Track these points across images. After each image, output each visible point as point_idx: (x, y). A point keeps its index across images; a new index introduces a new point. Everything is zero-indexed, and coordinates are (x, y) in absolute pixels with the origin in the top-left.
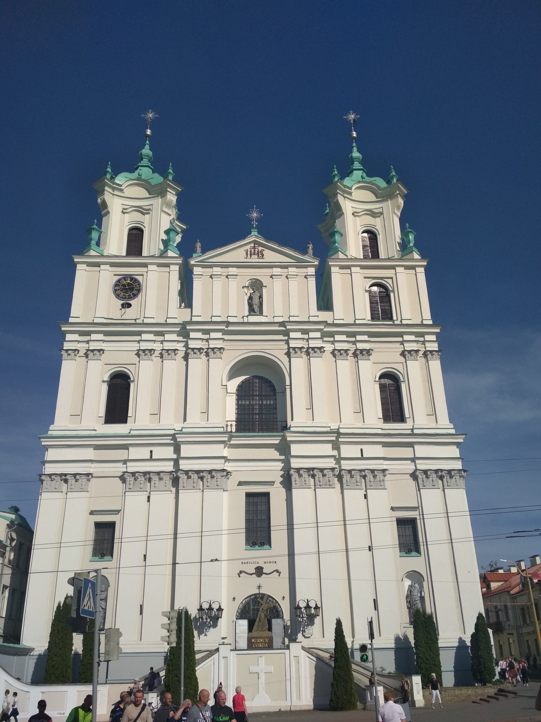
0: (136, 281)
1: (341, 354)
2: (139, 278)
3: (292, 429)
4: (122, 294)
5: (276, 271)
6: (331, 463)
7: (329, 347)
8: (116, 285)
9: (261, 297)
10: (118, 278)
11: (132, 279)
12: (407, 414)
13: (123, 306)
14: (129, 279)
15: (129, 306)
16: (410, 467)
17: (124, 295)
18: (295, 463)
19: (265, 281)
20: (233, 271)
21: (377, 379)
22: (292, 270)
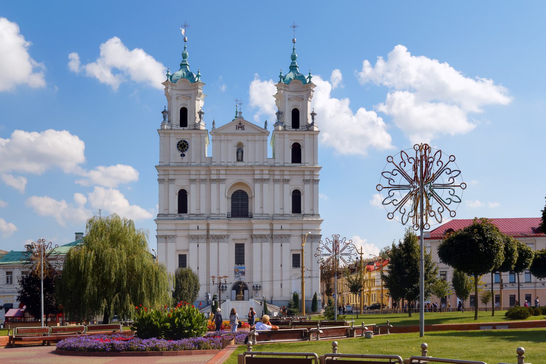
0: (186, 142)
1: (277, 181)
2: (187, 141)
3: (254, 218)
5: (250, 138)
6: (268, 233)
7: (272, 178)
8: (178, 144)
9: (242, 152)
11: (184, 141)
12: (302, 210)
13: (181, 155)
15: (184, 155)
16: (299, 233)
18: (255, 233)
19: (245, 143)
20: (230, 138)
21: (291, 193)
22: (257, 137)
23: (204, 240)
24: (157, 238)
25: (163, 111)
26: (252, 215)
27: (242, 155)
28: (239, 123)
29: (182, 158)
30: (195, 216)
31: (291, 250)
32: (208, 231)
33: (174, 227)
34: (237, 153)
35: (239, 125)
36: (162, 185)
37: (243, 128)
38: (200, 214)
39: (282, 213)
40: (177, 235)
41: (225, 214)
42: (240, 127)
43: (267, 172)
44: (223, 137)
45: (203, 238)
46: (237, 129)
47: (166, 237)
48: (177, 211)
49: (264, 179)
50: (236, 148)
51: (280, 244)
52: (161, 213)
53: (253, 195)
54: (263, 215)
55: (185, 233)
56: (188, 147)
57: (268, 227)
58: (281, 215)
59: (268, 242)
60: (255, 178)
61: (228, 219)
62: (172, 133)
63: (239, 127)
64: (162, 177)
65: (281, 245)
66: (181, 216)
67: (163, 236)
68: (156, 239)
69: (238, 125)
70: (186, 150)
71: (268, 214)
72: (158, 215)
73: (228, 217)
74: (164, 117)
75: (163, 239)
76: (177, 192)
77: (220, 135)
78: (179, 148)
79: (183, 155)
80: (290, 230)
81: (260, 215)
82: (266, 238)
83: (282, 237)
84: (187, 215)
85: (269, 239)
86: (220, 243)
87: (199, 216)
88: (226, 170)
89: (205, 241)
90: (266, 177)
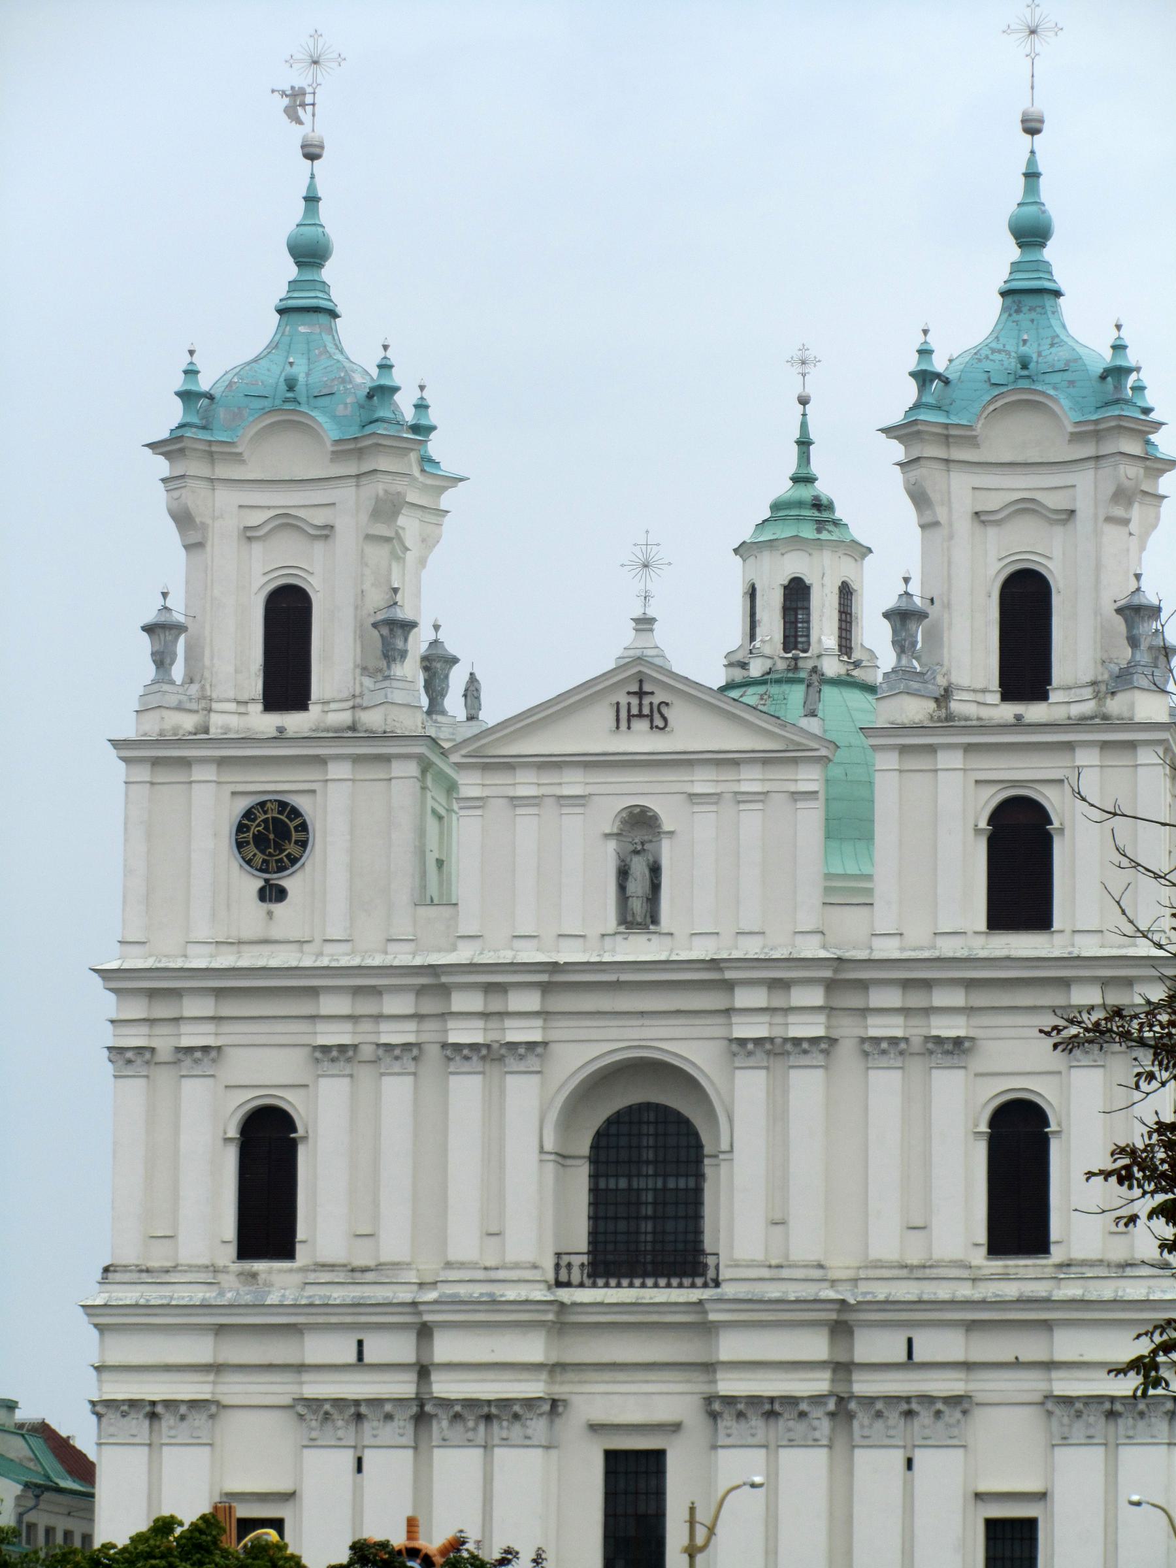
0: (295, 813)
2: (302, 803)
4: (260, 857)
5: (702, 782)
8: (241, 828)
9: (655, 870)
10: (243, 804)
11: (283, 805)
14: (275, 806)
17: (264, 861)
18: (730, 1385)
20: (573, 783)
22: (751, 780)
23: (401, 1429)
24: (99, 1416)
25: (150, 617)
26: (717, 1267)
27: (655, 887)
28: (635, 688)
29: (270, 914)
30: (340, 1277)
31: (979, 1496)
32: (423, 1371)
33: (201, 1350)
34: (623, 874)
35: (635, 701)
36: (135, 1088)
37: (659, 722)
38: (379, 1267)
39: (914, 1258)
40: (226, 1400)
41: (535, 1267)
42: (640, 715)
43: (815, 997)
44: (526, 784)
45: (389, 1417)
46: (624, 724)
47: (152, 1412)
48: (232, 1250)
49: (797, 1041)
50: (612, 845)
51: (898, 1457)
52: (130, 1255)
53: (724, 1146)
54: (785, 1273)
55: (282, 1389)
56: (304, 844)
57: (816, 1346)
58: (911, 1268)
59: (815, 1443)
60: (739, 1032)
61: (564, 1295)
62: (203, 760)
63: (635, 711)
64: (135, 1038)
65: (909, 1463)
66: (254, 1275)
67: (133, 1404)
68: (94, 1418)
69: (624, 700)
70: (294, 860)
71: (821, 1266)
72: (106, 1270)
73: (559, 1284)
74: (162, 660)
75: (138, 1425)
76: (233, 1132)
77: (509, 765)
78: (252, 850)
79: (272, 894)
80: (967, 1366)
81: (765, 1273)
82: (803, 1415)
83: (909, 1414)
84: (291, 1270)
85: (825, 1425)
86: (498, 1452)
87: (370, 1276)
88: (546, 988)
89: (408, 1440)
90: (811, 1028)
